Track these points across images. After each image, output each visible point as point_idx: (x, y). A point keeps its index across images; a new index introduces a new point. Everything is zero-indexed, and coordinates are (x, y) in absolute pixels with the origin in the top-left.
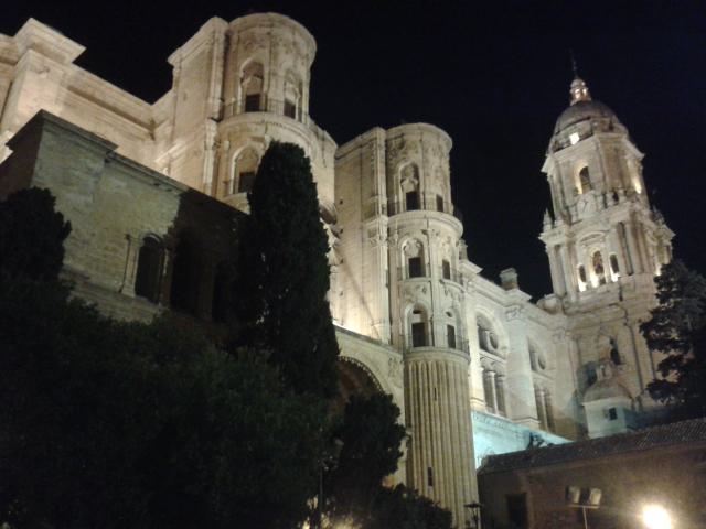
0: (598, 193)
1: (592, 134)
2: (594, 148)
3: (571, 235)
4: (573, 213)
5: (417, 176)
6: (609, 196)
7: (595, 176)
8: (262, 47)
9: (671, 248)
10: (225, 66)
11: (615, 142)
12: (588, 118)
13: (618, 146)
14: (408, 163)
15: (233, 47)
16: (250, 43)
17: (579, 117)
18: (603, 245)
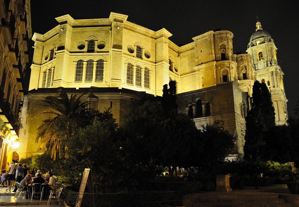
0: (265, 61)
1: (265, 42)
2: (265, 47)
3: (256, 73)
4: (257, 67)
5: (246, 69)
6: (269, 63)
7: (265, 56)
8: (225, 40)
9: (283, 78)
10: (214, 44)
11: (271, 45)
12: (263, 37)
13: (272, 47)
14: (243, 65)
15: (216, 39)
16: (221, 39)
17: (260, 36)
18: (265, 77)
